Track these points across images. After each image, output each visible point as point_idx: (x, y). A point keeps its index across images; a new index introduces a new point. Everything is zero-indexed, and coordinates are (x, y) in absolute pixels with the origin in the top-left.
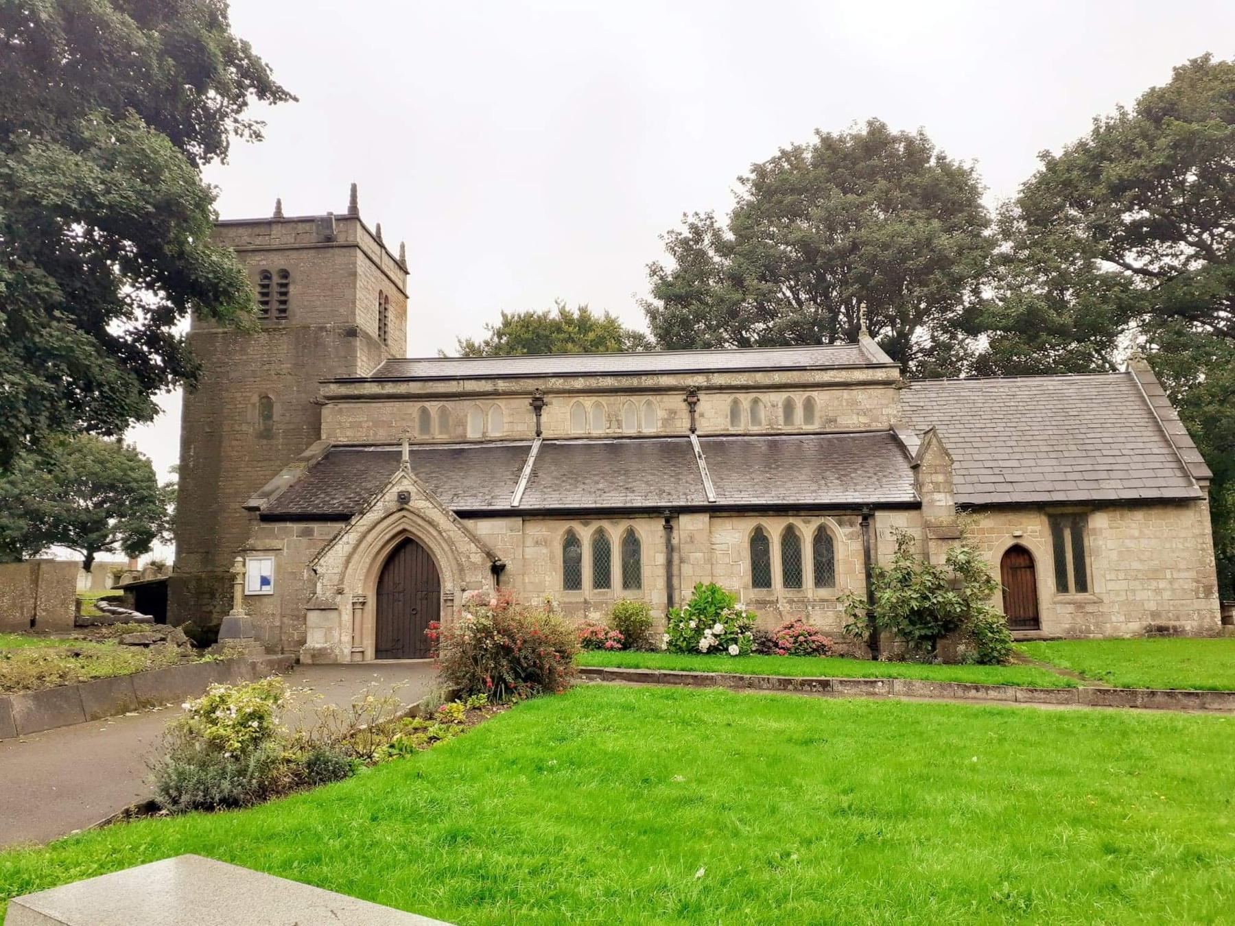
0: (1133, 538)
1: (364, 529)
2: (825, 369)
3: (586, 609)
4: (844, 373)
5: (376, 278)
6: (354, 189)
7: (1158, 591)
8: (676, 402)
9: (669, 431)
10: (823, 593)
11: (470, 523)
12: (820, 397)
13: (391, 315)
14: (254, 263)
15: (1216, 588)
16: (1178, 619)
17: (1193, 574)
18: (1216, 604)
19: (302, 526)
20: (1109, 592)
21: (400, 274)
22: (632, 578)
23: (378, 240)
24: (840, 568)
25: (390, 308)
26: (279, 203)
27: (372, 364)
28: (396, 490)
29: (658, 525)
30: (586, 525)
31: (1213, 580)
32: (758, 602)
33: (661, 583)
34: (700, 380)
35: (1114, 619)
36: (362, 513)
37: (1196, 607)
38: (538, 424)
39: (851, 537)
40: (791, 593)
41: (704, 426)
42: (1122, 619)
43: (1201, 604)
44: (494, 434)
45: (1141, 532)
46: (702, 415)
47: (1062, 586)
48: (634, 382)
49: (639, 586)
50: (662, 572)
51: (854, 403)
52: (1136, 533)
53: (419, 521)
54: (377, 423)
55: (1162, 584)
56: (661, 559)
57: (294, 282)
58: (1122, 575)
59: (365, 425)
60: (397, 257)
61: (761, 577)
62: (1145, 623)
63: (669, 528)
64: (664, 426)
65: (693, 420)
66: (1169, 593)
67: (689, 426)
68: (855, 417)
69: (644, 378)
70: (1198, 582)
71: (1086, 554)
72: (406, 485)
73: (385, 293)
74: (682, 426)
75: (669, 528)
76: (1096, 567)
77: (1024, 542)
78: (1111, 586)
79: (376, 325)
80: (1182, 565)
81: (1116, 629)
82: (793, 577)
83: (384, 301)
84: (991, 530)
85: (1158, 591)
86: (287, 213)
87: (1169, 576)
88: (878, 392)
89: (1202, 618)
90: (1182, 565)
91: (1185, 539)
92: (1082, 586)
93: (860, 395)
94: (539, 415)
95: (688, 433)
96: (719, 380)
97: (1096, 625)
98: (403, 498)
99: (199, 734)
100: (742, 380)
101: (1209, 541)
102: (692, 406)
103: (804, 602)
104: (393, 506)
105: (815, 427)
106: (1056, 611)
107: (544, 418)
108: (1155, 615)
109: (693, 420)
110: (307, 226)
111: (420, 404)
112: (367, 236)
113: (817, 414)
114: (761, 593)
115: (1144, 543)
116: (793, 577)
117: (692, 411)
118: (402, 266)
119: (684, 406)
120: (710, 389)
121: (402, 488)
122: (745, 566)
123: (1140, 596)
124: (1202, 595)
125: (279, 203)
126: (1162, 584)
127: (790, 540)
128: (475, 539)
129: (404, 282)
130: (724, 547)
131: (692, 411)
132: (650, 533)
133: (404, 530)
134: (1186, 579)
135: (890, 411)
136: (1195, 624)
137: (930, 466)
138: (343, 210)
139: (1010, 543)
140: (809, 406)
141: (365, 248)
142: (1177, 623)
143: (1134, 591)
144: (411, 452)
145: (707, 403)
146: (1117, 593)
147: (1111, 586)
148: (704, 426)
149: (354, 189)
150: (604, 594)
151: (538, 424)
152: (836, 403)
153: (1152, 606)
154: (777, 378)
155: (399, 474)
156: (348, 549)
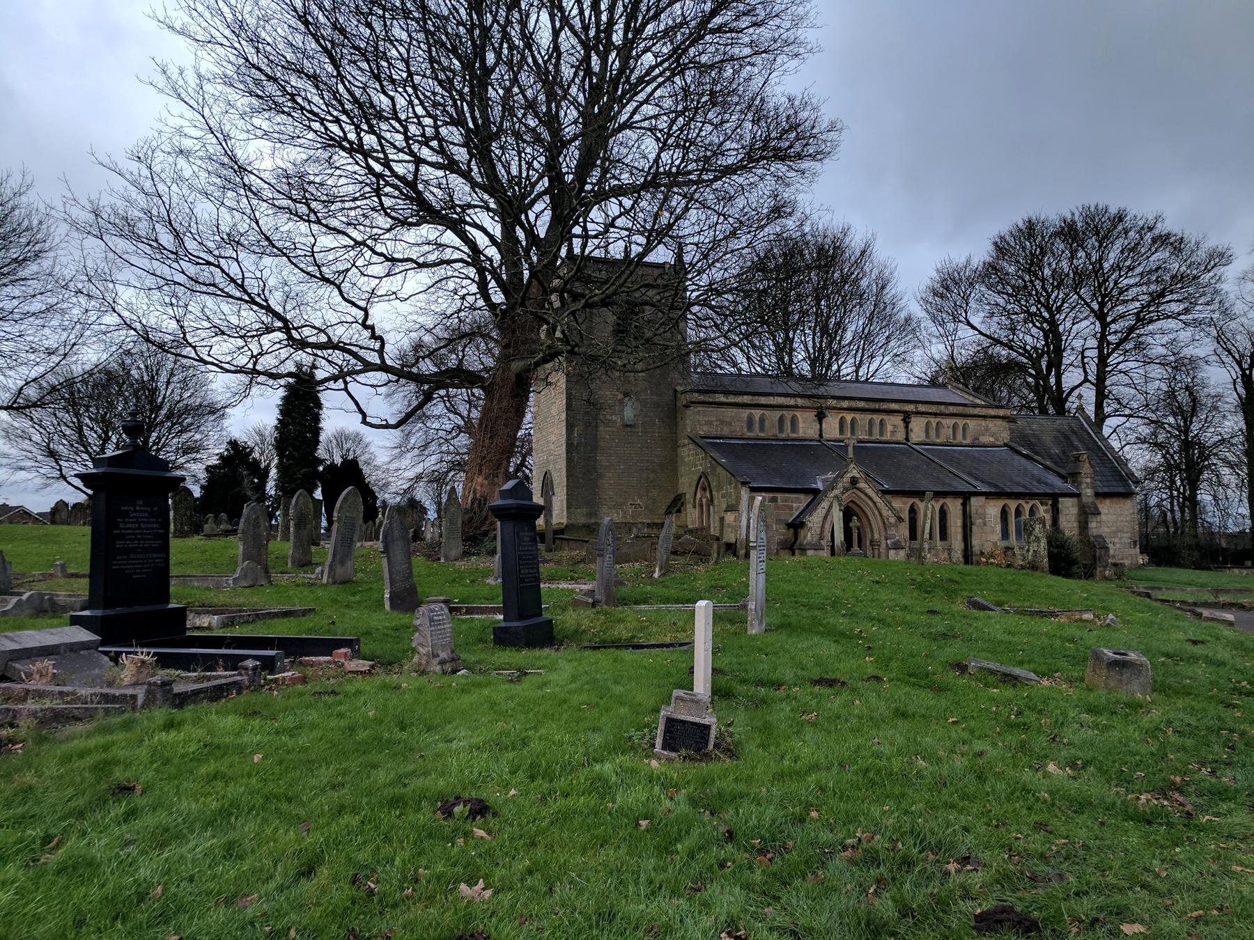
8: (897, 420)
9: (894, 439)
11: (888, 497)
12: (972, 423)
19: (771, 495)
28: (849, 475)
29: (959, 502)
33: (960, 537)
34: (911, 408)
48: (877, 406)
51: (987, 429)
53: (862, 496)
54: (722, 422)
56: (959, 522)
65: (907, 434)
72: (855, 473)
74: (900, 436)
88: (999, 422)
93: (991, 424)
94: (821, 424)
96: (922, 408)
98: (854, 481)
99: (438, 656)
100: (933, 409)
102: (906, 421)
109: (907, 434)
111: (748, 411)
117: (907, 427)
119: (901, 423)
120: (918, 413)
128: (892, 508)
131: (907, 427)
132: (954, 506)
145: (917, 424)
154: (952, 409)
156: (824, 511)
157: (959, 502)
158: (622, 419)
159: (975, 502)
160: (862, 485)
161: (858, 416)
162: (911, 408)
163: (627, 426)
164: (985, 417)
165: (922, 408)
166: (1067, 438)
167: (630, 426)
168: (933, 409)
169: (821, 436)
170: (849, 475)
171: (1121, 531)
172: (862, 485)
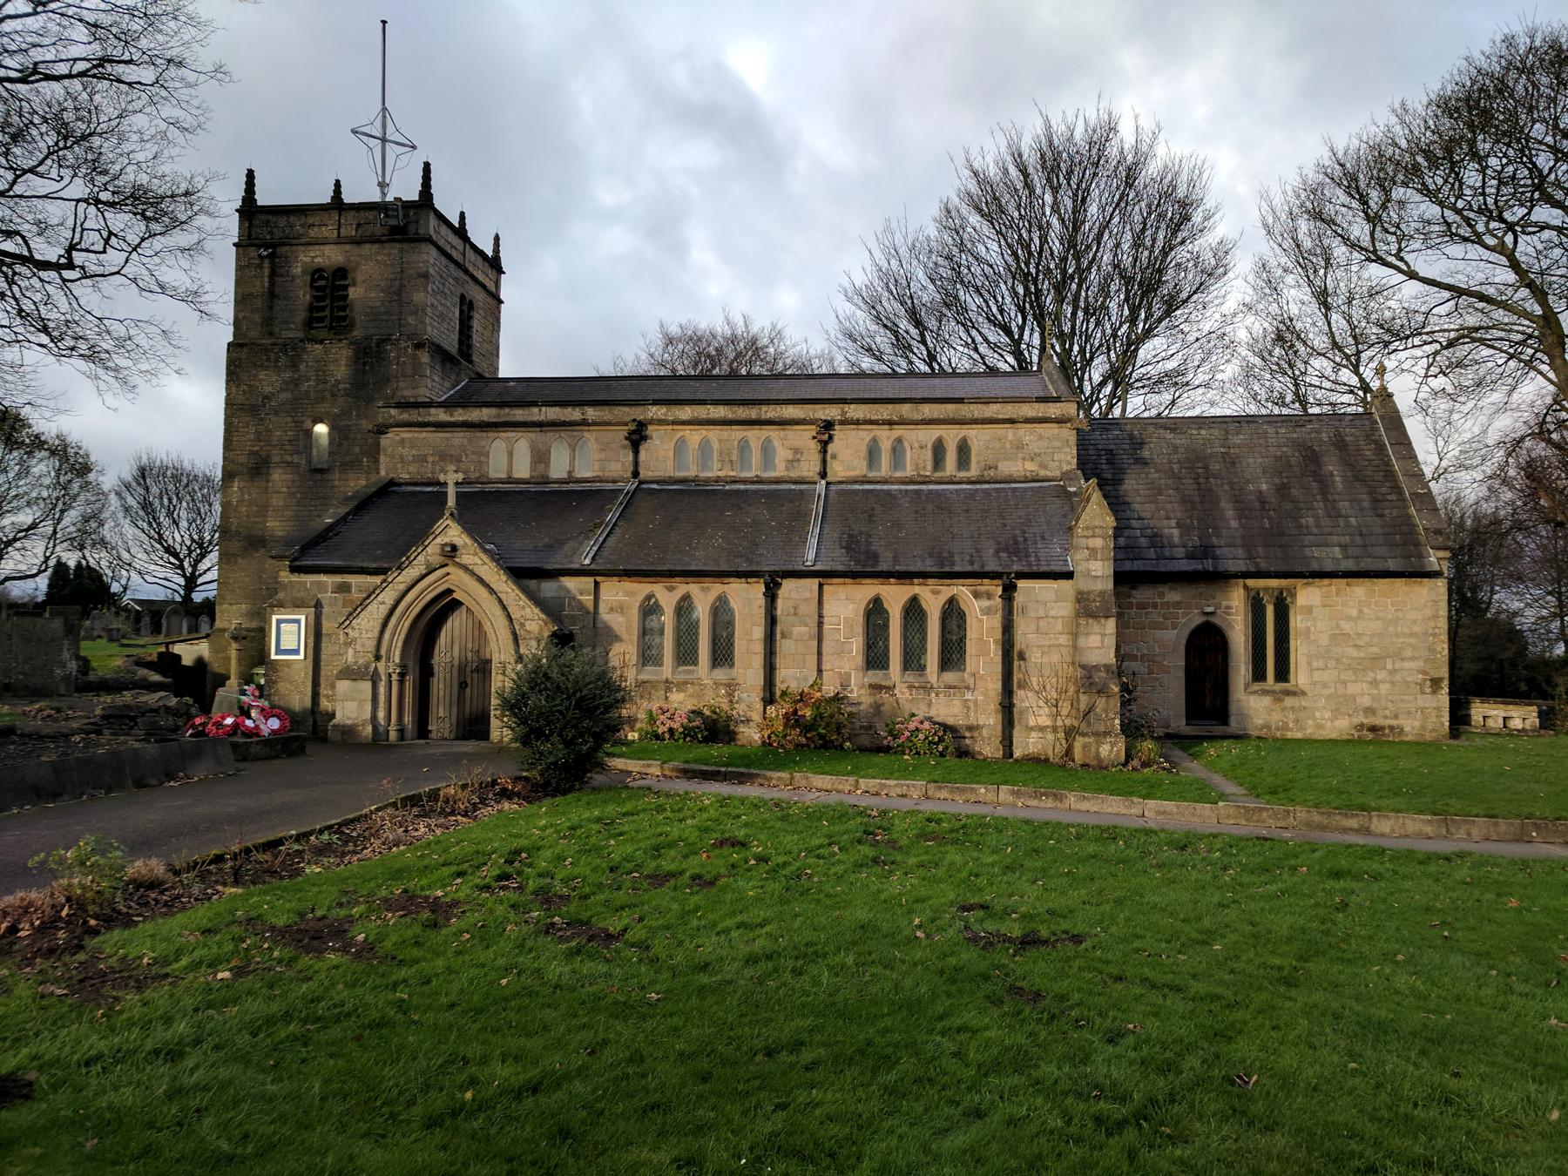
0: (1349, 618)
1: (402, 587)
2: (987, 401)
3: (668, 689)
4: (1009, 406)
5: (456, 279)
6: (250, 175)
7: (1375, 683)
8: (805, 438)
9: (794, 474)
10: (950, 677)
12: (978, 437)
13: (476, 324)
14: (307, 259)
15: (1446, 683)
16: (1396, 717)
17: (1420, 664)
18: (1444, 698)
19: (338, 579)
20: (1314, 683)
21: (492, 274)
22: (722, 654)
23: (461, 232)
24: (971, 647)
25: (476, 316)
26: (338, 184)
27: (447, 384)
30: (671, 589)
31: (1444, 672)
32: (871, 686)
33: (758, 661)
34: (832, 412)
35: (1318, 714)
36: (401, 568)
38: (636, 463)
39: (987, 611)
40: (911, 677)
41: (838, 470)
42: (1328, 715)
44: (583, 473)
45: (1360, 611)
46: (834, 457)
47: (1259, 674)
49: (732, 666)
50: (759, 647)
51: (1019, 446)
52: (1354, 613)
56: (759, 632)
57: (354, 284)
58: (1331, 664)
59: (430, 459)
60: (490, 254)
61: (875, 658)
62: (1356, 721)
63: (771, 595)
64: (787, 469)
65: (824, 462)
66: (1388, 686)
67: (817, 469)
68: (1020, 463)
69: (764, 408)
70: (1424, 673)
71: (1292, 637)
73: (468, 298)
74: (809, 467)
75: (771, 595)
76: (1299, 651)
77: (1216, 620)
78: (1317, 676)
79: (456, 337)
80: (1408, 653)
81: (1319, 727)
82: (912, 661)
83: (467, 306)
84: (1178, 605)
85: (1375, 683)
86: (348, 197)
87: (1389, 667)
88: (1052, 429)
89: (1425, 718)
90: (1408, 653)
91: (1414, 622)
92: (1283, 673)
94: (636, 452)
95: (817, 478)
97: (1296, 721)
101: (1443, 624)
102: (824, 445)
103: (927, 688)
104: (436, 560)
105: (974, 472)
106: (1254, 706)
107: (643, 456)
108: (1369, 711)
109: (824, 462)
110: (371, 215)
112: (444, 230)
113: (974, 459)
114: (875, 676)
115: (1362, 626)
116: (912, 661)
118: (495, 264)
119: (814, 446)
121: (446, 540)
122: (857, 645)
123: (1352, 689)
124: (1428, 690)
125: (338, 184)
126: (1381, 675)
127: (914, 611)
129: (497, 284)
130: (834, 620)
132: (746, 598)
133: (449, 592)
134: (1411, 670)
135: (1062, 456)
136: (1417, 724)
137: (1087, 528)
138: (412, 194)
139: (1199, 620)
140: (964, 450)
141: (441, 243)
142: (1394, 722)
143: (1344, 683)
144: (459, 495)
146: (1325, 685)
147: (1317, 676)
148: (838, 470)
149: (250, 175)
150: (689, 672)
151: (636, 463)
152: (998, 445)
153: (1366, 701)
155: (442, 524)
156: (384, 610)
157: (758, 589)
158: (310, 462)
159: (790, 590)
160: (466, 558)
161: (713, 433)
162: (832, 412)
163: (317, 471)
164: (1012, 421)
165: (855, 411)
166: (1312, 458)
167: (321, 471)
168: (884, 412)
169: (636, 474)
170: (439, 540)
172: (466, 558)
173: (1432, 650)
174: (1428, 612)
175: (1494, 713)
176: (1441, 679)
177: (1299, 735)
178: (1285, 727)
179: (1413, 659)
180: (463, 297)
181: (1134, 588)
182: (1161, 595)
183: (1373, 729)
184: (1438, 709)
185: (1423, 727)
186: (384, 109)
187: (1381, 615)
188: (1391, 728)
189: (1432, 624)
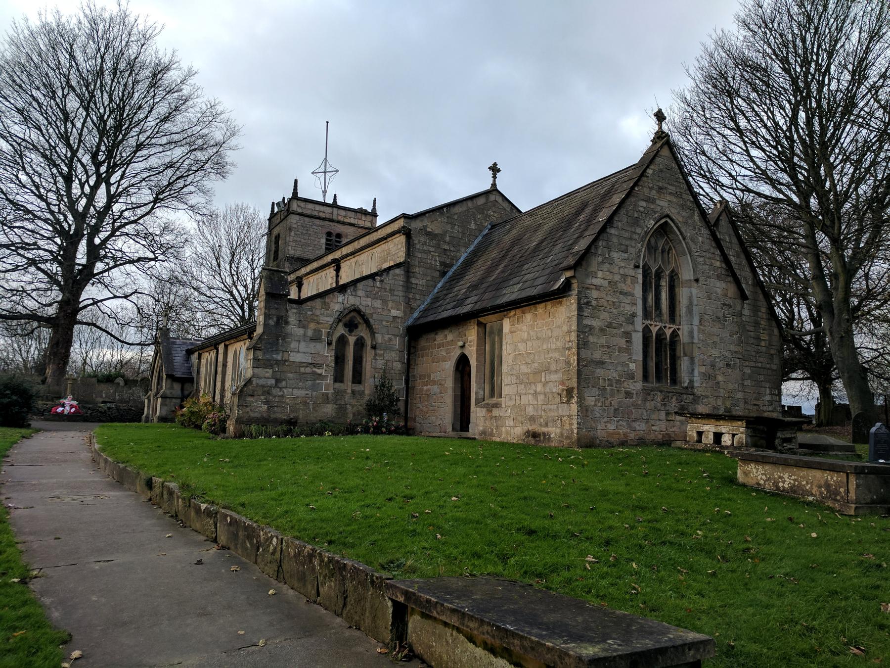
16: (547, 425)
23: (334, 205)
37: (560, 413)
43: (564, 410)
55: (539, 388)
70: (562, 383)
80: (553, 367)
85: (535, 394)
108: (532, 419)
123: (525, 400)
136: (558, 431)
142: (545, 430)
171: (547, 370)
173: (568, 363)
174: (565, 328)
175: (706, 428)
176: (573, 388)
177: (498, 440)
178: (492, 434)
179: (557, 371)
180: (329, 234)
181: (436, 334)
182: (446, 336)
183: (535, 435)
184: (570, 416)
185: (562, 434)
186: (326, 159)
187: (539, 335)
188: (544, 434)
189: (568, 339)
